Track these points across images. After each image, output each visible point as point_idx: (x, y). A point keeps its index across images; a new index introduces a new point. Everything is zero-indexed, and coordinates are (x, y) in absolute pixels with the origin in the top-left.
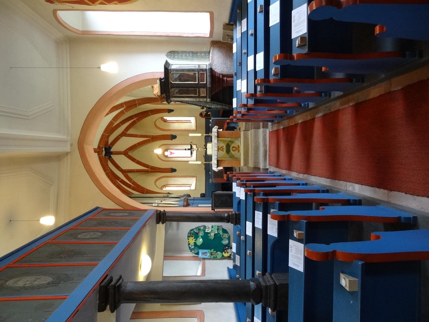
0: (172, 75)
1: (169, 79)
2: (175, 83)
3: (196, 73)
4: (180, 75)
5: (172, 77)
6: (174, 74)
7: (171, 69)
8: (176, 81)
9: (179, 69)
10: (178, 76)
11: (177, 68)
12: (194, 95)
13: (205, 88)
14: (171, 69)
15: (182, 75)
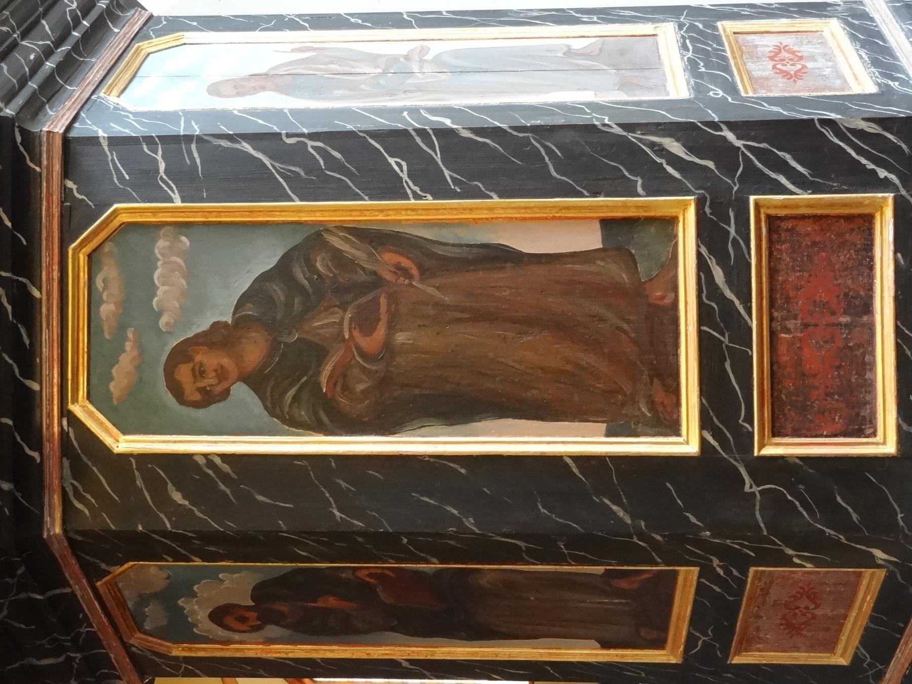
0: (109, 272)
1: (30, 367)
2: (186, 459)
3: (669, 223)
4: (282, 270)
5: (106, 309)
6: (162, 244)
7: (94, 141)
8: (208, 398)
9: (255, 138)
10: (243, 284)
11: (236, 104)
12: (606, 645)
13: (871, 563)
14: (88, 127)
15: (337, 256)
